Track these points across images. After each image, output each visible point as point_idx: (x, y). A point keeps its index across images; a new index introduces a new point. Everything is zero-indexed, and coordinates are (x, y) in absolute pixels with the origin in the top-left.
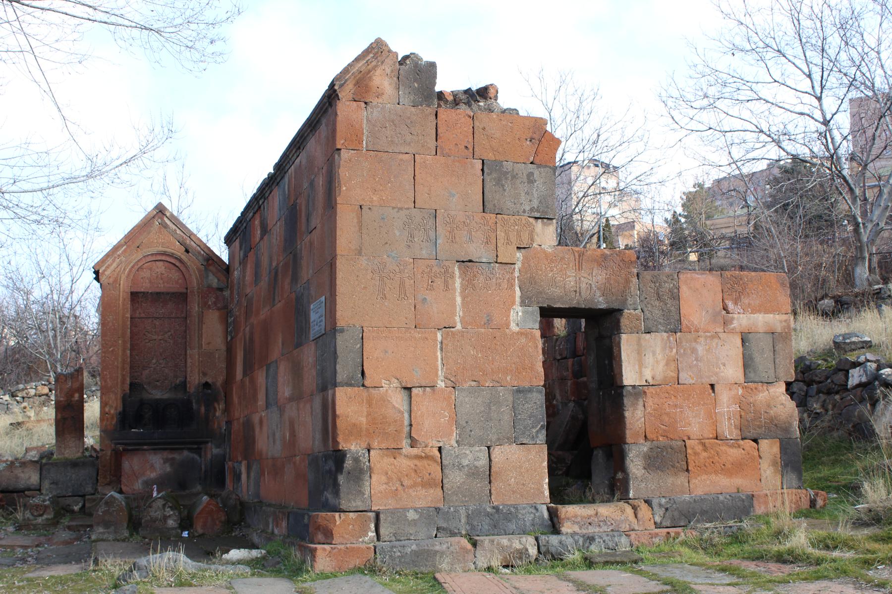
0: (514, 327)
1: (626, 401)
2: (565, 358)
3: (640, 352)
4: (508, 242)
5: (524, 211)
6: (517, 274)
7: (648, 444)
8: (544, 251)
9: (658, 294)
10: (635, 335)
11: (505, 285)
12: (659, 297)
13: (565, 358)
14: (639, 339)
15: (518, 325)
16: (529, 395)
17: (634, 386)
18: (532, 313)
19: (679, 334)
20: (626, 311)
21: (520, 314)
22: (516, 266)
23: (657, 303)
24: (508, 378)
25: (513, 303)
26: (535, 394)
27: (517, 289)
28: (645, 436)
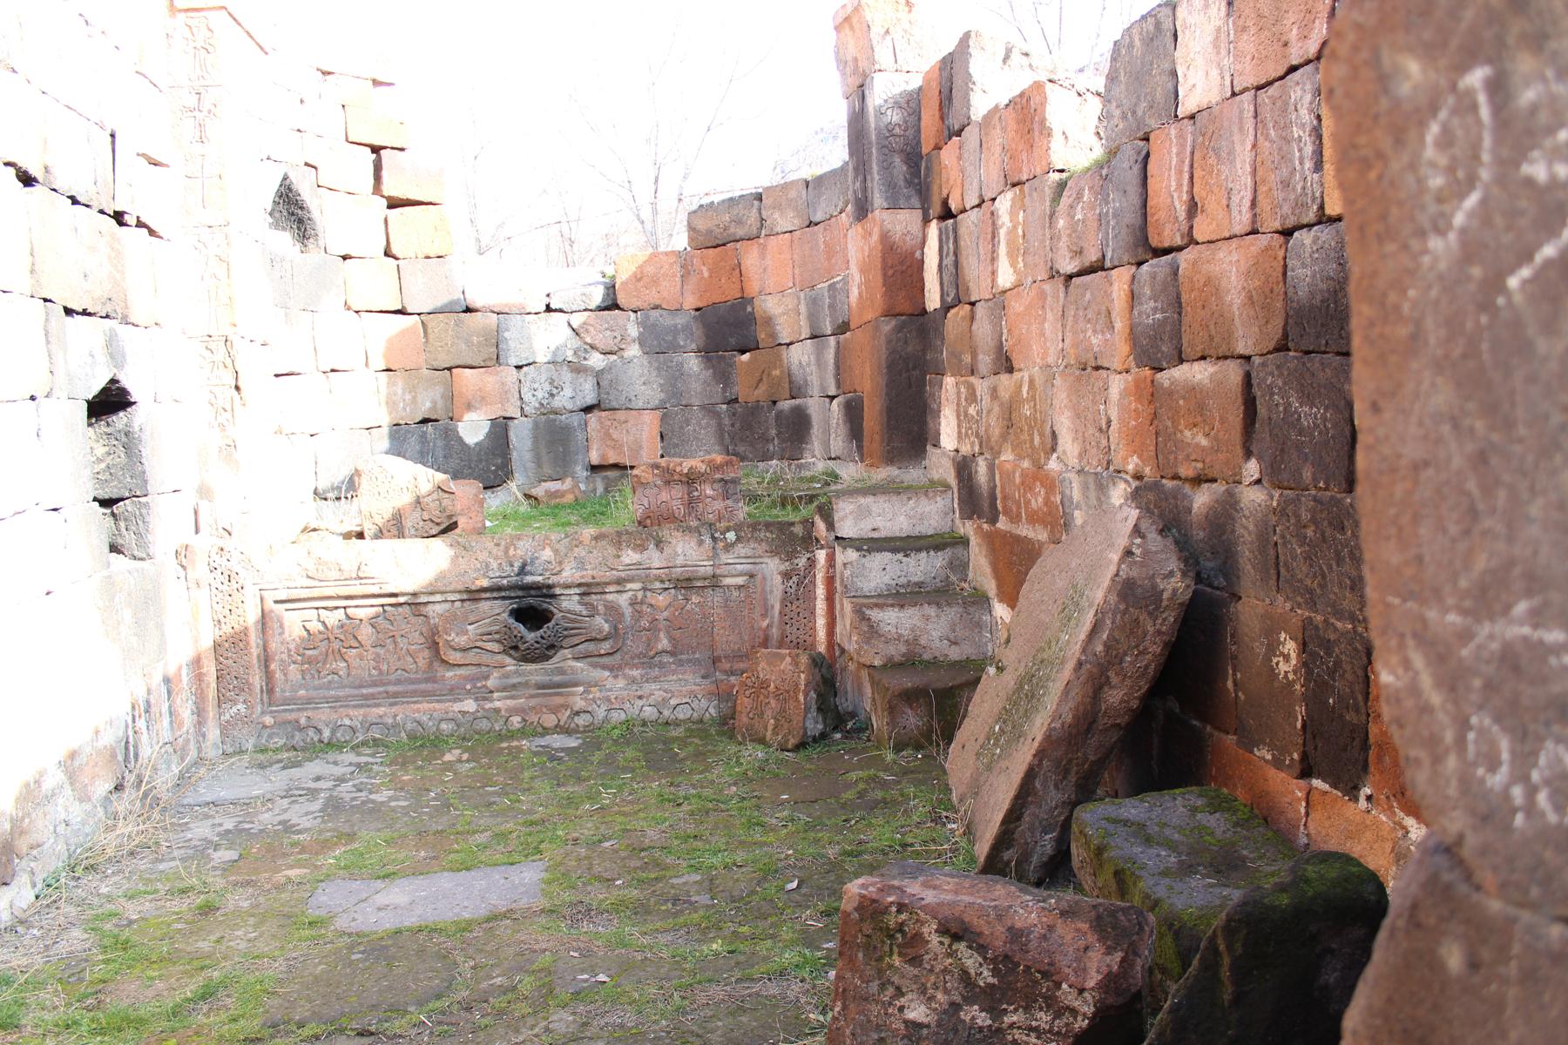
2: (1097, 267)
13: (1097, 267)
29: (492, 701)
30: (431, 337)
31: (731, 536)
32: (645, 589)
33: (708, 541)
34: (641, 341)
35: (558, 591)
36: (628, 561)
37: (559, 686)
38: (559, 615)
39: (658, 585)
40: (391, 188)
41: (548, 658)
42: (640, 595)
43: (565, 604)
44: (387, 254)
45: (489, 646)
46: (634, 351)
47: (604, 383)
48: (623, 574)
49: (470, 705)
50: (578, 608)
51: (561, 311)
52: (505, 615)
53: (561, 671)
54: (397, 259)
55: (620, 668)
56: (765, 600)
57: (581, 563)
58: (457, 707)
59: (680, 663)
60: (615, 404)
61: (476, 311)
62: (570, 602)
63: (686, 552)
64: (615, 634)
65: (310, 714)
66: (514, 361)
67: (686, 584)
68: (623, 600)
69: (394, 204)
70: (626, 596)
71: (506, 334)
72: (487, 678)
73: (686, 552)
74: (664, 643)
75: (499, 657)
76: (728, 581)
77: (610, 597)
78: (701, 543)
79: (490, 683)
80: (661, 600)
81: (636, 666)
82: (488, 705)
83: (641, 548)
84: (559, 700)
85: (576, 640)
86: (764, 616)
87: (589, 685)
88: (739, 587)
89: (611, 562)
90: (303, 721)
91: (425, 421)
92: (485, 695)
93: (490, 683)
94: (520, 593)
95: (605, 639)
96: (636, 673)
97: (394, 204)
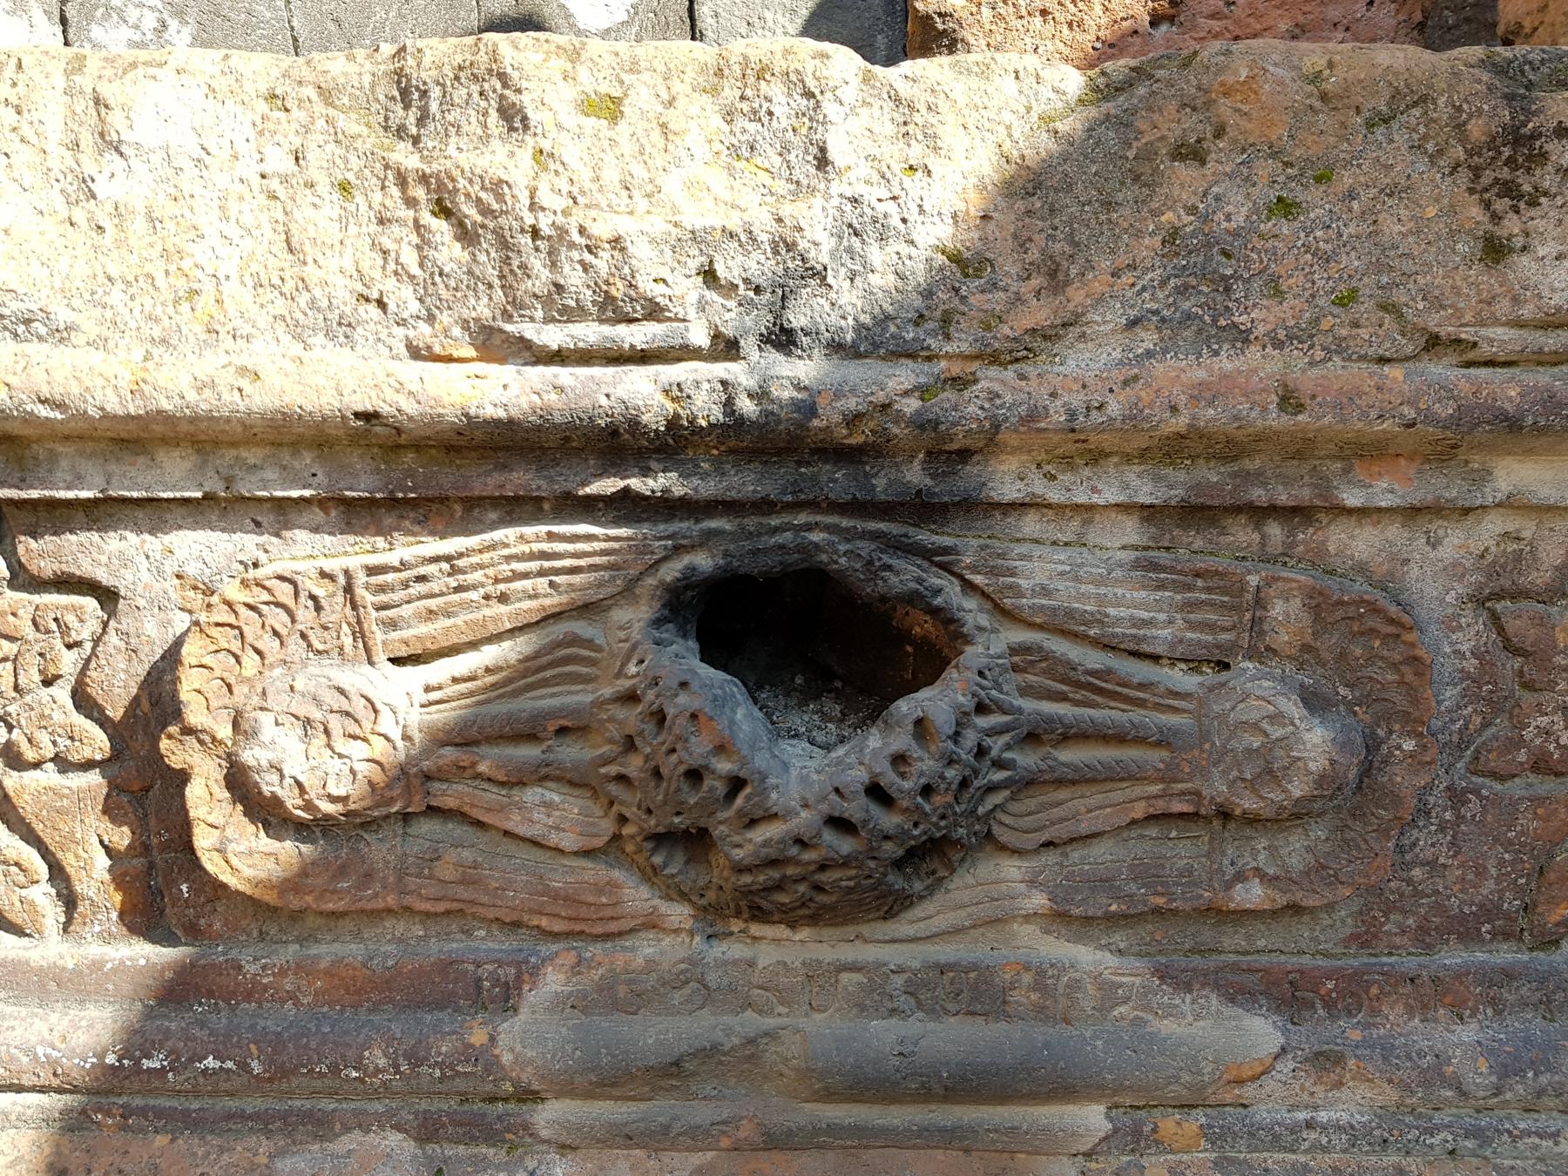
35: (1006, 479)
38: (990, 643)
41: (893, 905)
43: (1043, 569)
48: (1508, 389)
50: (1131, 604)
52: (634, 617)
53: (976, 992)
55: (1352, 994)
57: (1206, 288)
62: (1069, 564)
64: (1356, 792)
68: (1435, 571)
70: (1456, 542)
72: (504, 998)
75: (594, 871)
77: (1358, 544)
81: (1441, 995)
89: (1451, 285)
93: (522, 1038)
94: (745, 483)
95: (1296, 815)
96: (1462, 1040)
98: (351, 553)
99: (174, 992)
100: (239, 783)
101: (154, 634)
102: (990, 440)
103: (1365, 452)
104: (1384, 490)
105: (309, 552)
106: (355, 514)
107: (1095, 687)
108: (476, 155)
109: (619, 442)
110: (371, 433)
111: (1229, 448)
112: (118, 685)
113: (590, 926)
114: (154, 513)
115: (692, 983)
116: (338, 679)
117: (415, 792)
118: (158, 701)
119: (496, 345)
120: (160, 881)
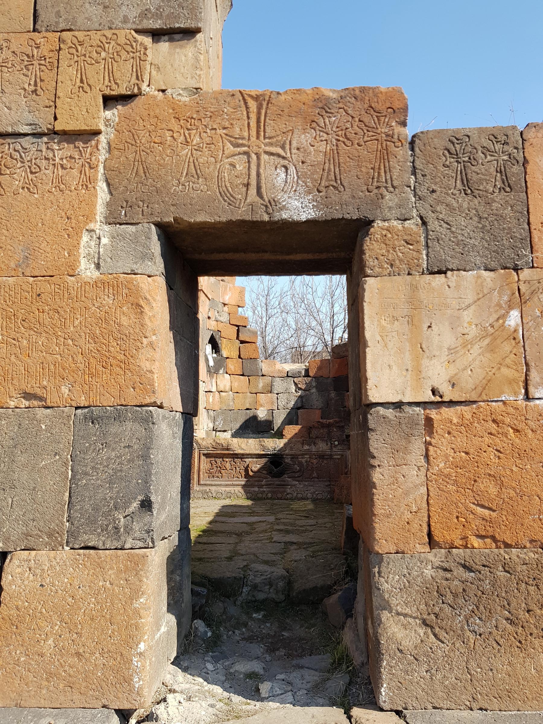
0: (87, 270)
1: (377, 443)
3: (415, 317)
4: (84, 84)
5: (125, 20)
6: (103, 155)
7: (437, 557)
8: (174, 106)
9: (466, 182)
10: (402, 280)
11: (73, 177)
12: (468, 187)
14: (414, 288)
15: (98, 266)
16: (114, 428)
17: (398, 405)
18: (135, 239)
19: (526, 273)
20: (379, 223)
21: (105, 241)
22: (102, 138)
23: (465, 202)
24: (65, 390)
25: (90, 217)
26: (129, 425)
27: (102, 186)
28: (430, 535)
29: (263, 488)
30: (251, 383)
31: (336, 443)
32: (310, 458)
33: (329, 444)
34: (316, 387)
36: (305, 449)
37: (283, 485)
39: (314, 457)
40: (242, 338)
42: (309, 459)
44: (240, 357)
45: (264, 472)
46: (314, 390)
47: (304, 400)
49: (256, 489)
50: (290, 462)
51: (291, 377)
54: (242, 359)
56: (346, 463)
57: (291, 449)
58: (252, 489)
59: (320, 481)
60: (307, 407)
61: (265, 376)
62: (288, 460)
63: (322, 446)
65: (210, 488)
66: (276, 392)
67: (322, 456)
68: (303, 460)
69: (242, 342)
71: (274, 384)
73: (322, 446)
74: (315, 475)
76: (335, 457)
77: (300, 459)
78: (327, 444)
79: (263, 483)
80: (315, 461)
82: (262, 490)
83: (309, 445)
84: (281, 490)
85: (289, 472)
86: (346, 468)
87: (292, 486)
88: (338, 459)
90: (208, 490)
91: (247, 409)
92: (260, 486)
93: (263, 483)
95: (298, 472)
96: (306, 483)
97: (242, 342)
98: (257, 460)
99: (247, 481)
100: (251, 470)
101: (248, 463)
102: (283, 455)
103: (299, 455)
104: (300, 457)
105: (255, 460)
106: (257, 458)
107: (289, 466)
108: (263, 443)
109: (268, 455)
110: (258, 454)
111: (293, 455)
112: (245, 466)
113: (266, 478)
114: (248, 458)
115: (271, 481)
116: (256, 465)
117: (259, 471)
118: (248, 466)
119: (263, 451)
120: (247, 475)
